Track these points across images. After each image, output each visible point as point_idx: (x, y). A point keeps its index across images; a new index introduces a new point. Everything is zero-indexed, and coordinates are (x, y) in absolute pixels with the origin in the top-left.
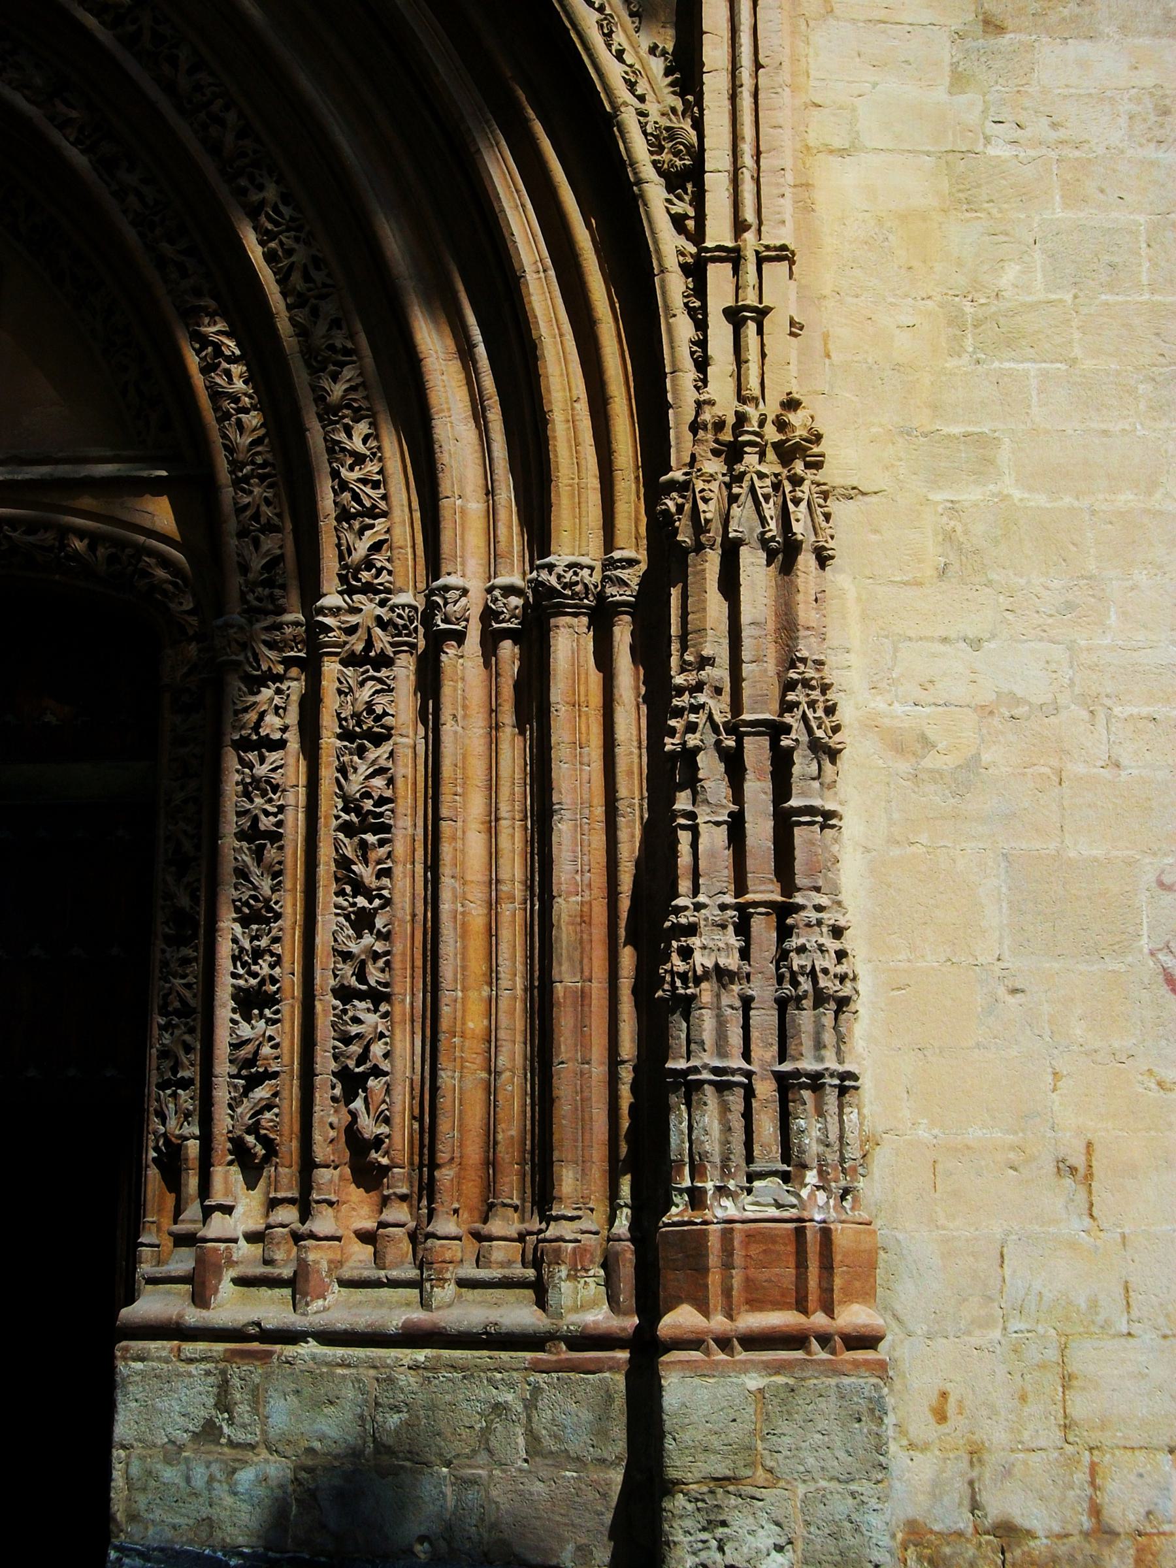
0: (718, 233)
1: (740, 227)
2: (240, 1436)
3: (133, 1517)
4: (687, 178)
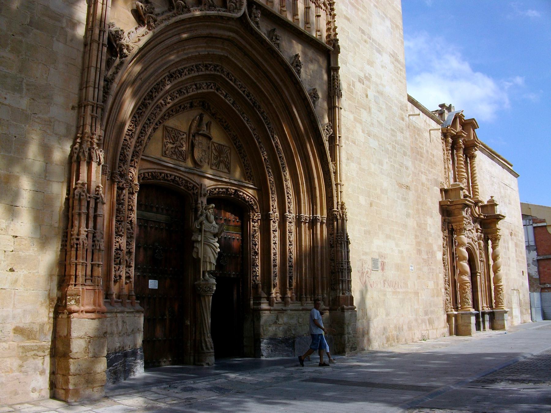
0: (339, 182)
1: (340, 181)
2: (280, 323)
3: (264, 335)
4: (335, 173)
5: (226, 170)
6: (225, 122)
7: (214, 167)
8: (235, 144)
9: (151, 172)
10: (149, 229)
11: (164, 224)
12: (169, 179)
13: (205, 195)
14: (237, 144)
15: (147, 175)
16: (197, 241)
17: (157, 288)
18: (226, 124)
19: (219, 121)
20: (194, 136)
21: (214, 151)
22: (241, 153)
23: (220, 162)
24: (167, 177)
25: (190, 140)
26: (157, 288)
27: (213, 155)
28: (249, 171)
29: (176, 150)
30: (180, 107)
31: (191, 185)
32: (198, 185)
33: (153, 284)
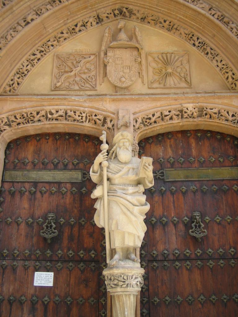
5: (184, 85)
6: (165, 21)
7: (156, 85)
8: (194, 45)
9: (20, 113)
10: (38, 195)
11: (68, 185)
12: (55, 116)
13: (126, 126)
14: (197, 43)
15: (13, 118)
16: (96, 200)
17: (51, 284)
18: (167, 23)
19: (156, 24)
20: (106, 54)
21: (154, 65)
22: (207, 54)
23: (167, 75)
24: (51, 114)
25: (101, 61)
26: (51, 284)
27: (151, 70)
28: (230, 74)
29: (78, 79)
30: (76, 26)
31: (101, 117)
32: (114, 114)
33: (44, 279)
